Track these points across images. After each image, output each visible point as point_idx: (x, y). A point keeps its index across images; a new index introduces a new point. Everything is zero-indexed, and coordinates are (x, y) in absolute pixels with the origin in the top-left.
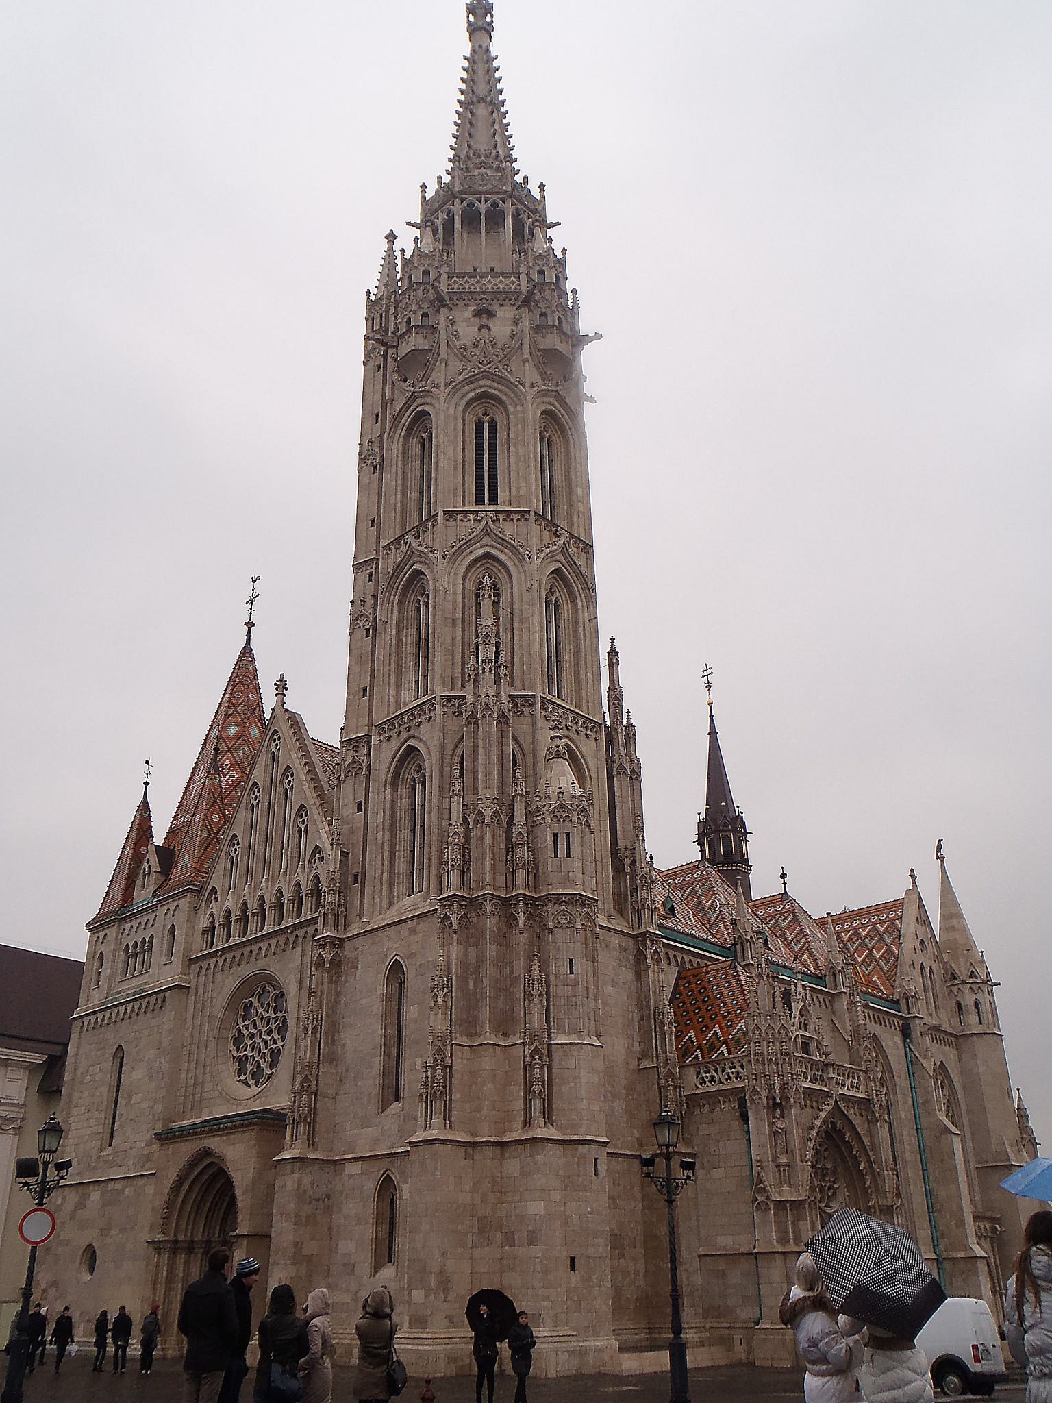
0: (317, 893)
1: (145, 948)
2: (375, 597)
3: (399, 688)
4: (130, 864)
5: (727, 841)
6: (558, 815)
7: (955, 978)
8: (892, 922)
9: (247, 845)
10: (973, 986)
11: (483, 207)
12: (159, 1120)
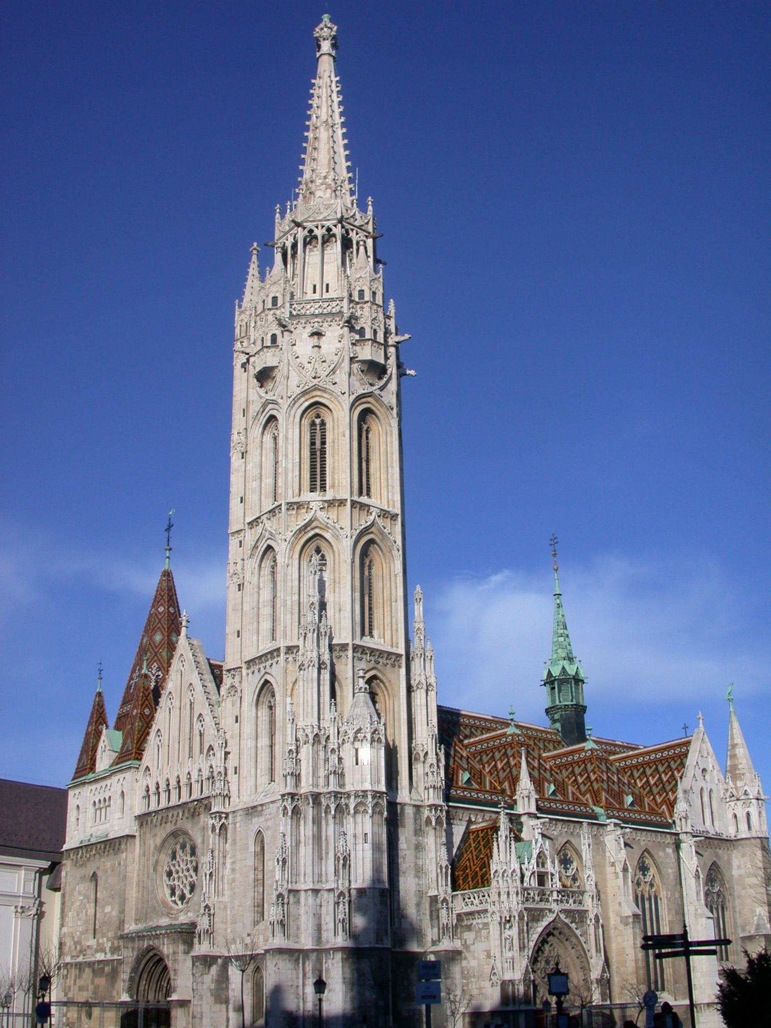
11: (319, 233)
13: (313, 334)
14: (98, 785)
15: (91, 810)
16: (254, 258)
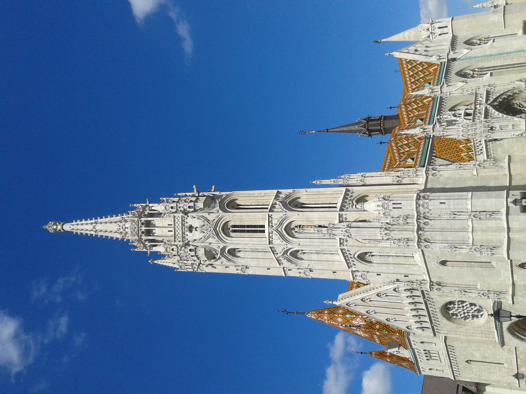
2: (298, 269)
5: (374, 125)
6: (386, 207)
7: (429, 36)
8: (407, 63)
9: (390, 315)
10: (432, 30)
11: (143, 228)
13: (191, 231)
14: (418, 357)
15: (431, 362)
16: (156, 262)
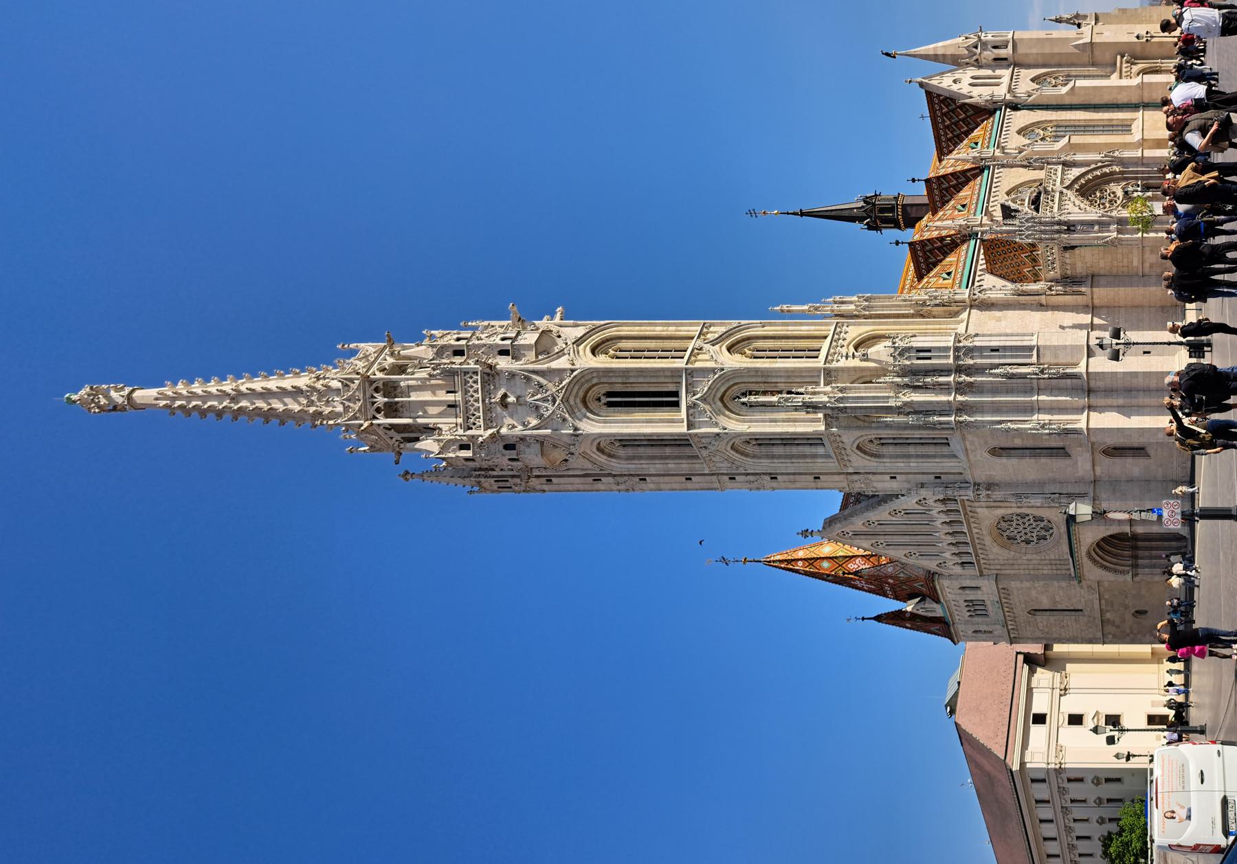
0: (943, 501)
1: (970, 604)
2: (748, 474)
3: (814, 456)
4: (918, 622)
9: (912, 547)
12: (1069, 583)
